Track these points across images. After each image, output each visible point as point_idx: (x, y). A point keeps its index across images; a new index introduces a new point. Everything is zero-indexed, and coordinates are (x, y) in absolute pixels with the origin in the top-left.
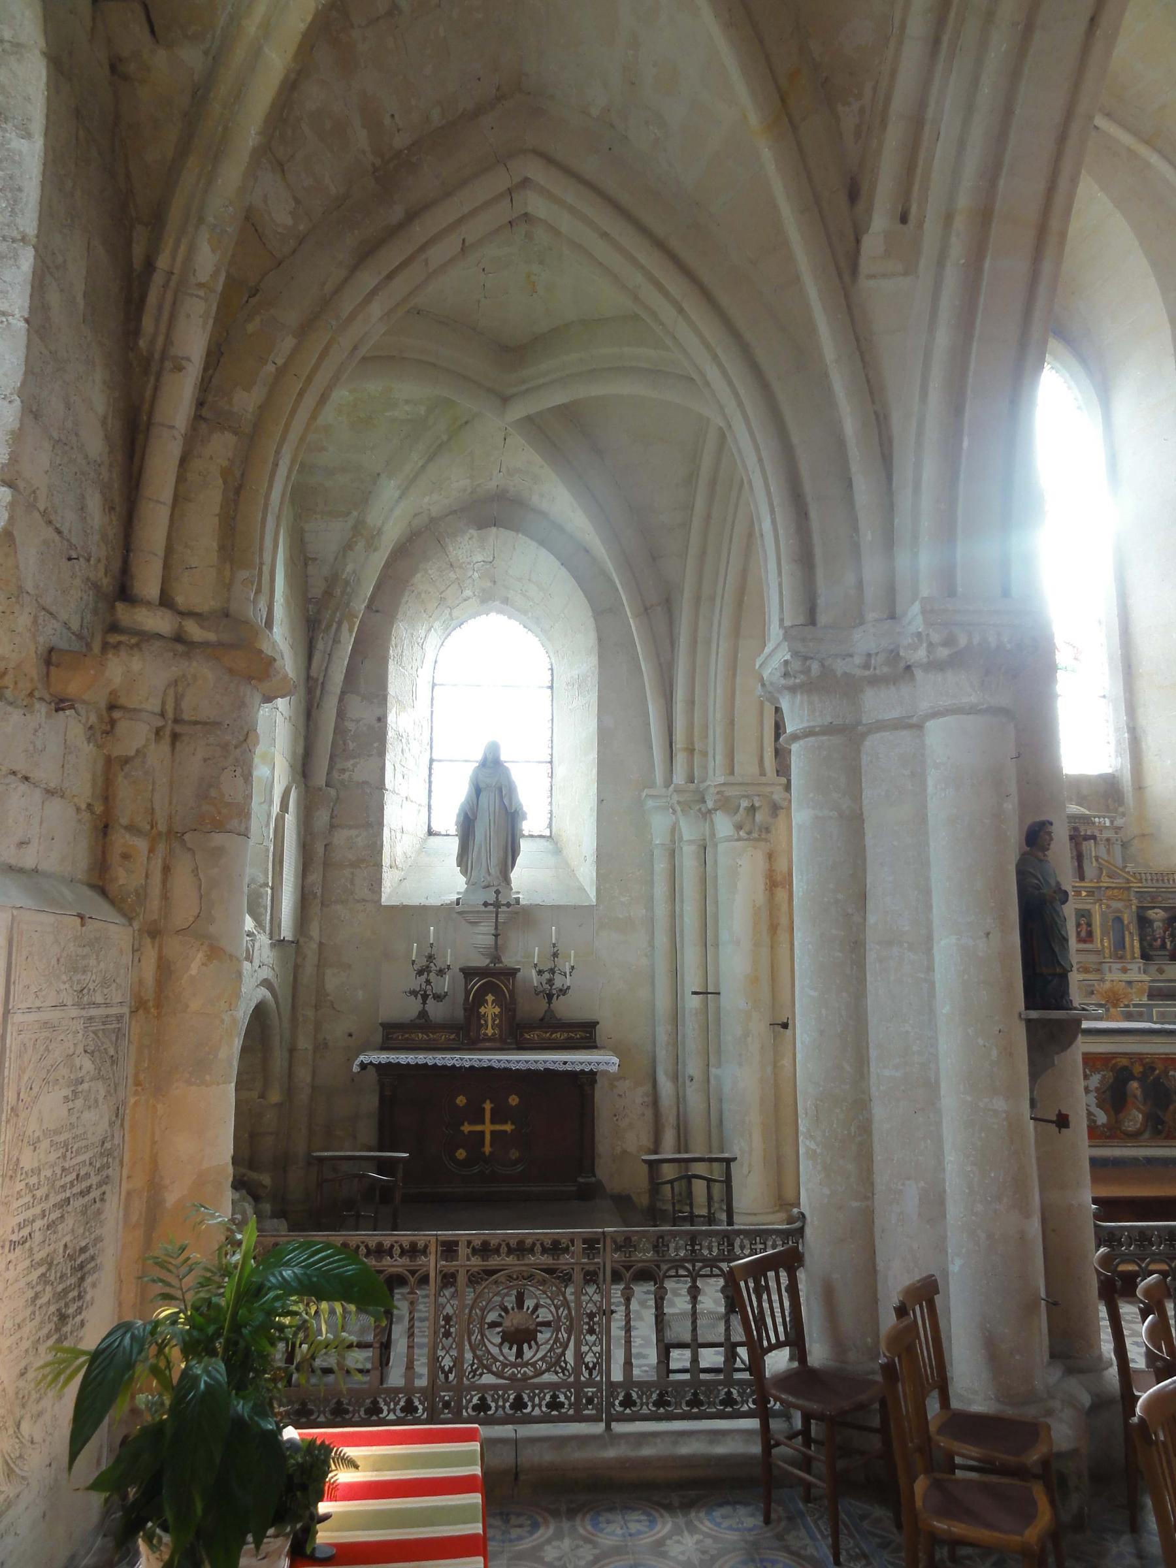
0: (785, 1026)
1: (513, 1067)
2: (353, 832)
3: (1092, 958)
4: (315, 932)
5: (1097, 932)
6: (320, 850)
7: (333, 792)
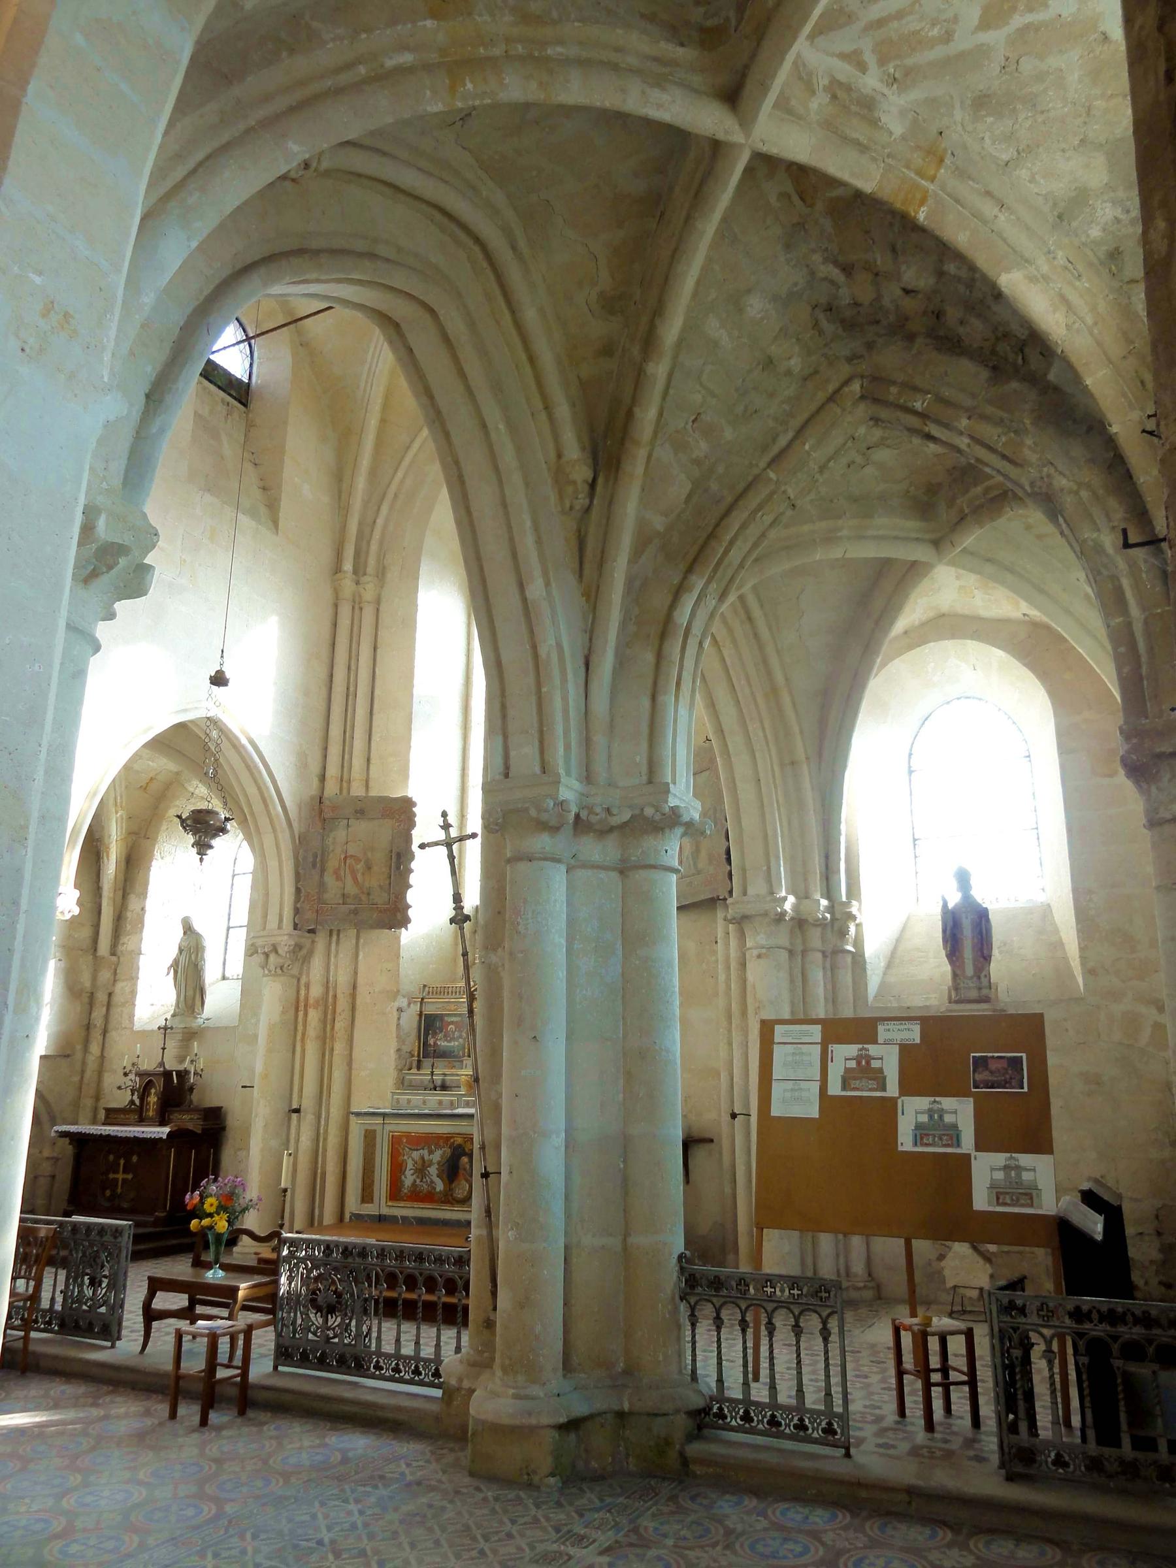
0: (297, 1111)
1: (120, 1135)
2: (124, 984)
4: (95, 1049)
6: (101, 997)
7: (114, 959)
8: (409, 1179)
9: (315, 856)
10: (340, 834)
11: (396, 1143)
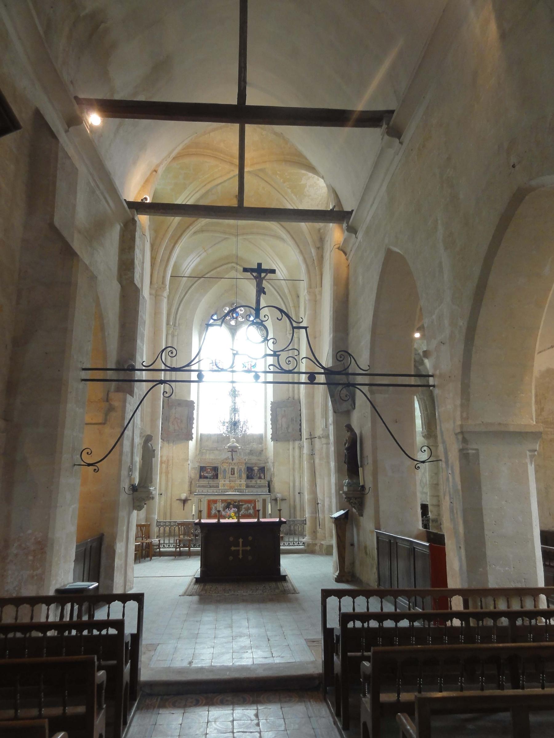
0: (161, 494)
3: (234, 479)
5: (236, 472)
8: (213, 512)
9: (167, 417)
10: (173, 411)
11: (210, 503)
